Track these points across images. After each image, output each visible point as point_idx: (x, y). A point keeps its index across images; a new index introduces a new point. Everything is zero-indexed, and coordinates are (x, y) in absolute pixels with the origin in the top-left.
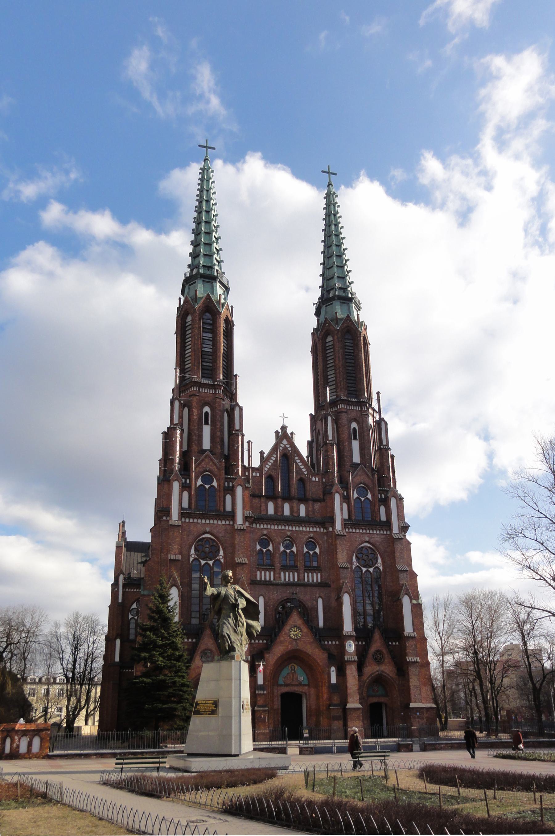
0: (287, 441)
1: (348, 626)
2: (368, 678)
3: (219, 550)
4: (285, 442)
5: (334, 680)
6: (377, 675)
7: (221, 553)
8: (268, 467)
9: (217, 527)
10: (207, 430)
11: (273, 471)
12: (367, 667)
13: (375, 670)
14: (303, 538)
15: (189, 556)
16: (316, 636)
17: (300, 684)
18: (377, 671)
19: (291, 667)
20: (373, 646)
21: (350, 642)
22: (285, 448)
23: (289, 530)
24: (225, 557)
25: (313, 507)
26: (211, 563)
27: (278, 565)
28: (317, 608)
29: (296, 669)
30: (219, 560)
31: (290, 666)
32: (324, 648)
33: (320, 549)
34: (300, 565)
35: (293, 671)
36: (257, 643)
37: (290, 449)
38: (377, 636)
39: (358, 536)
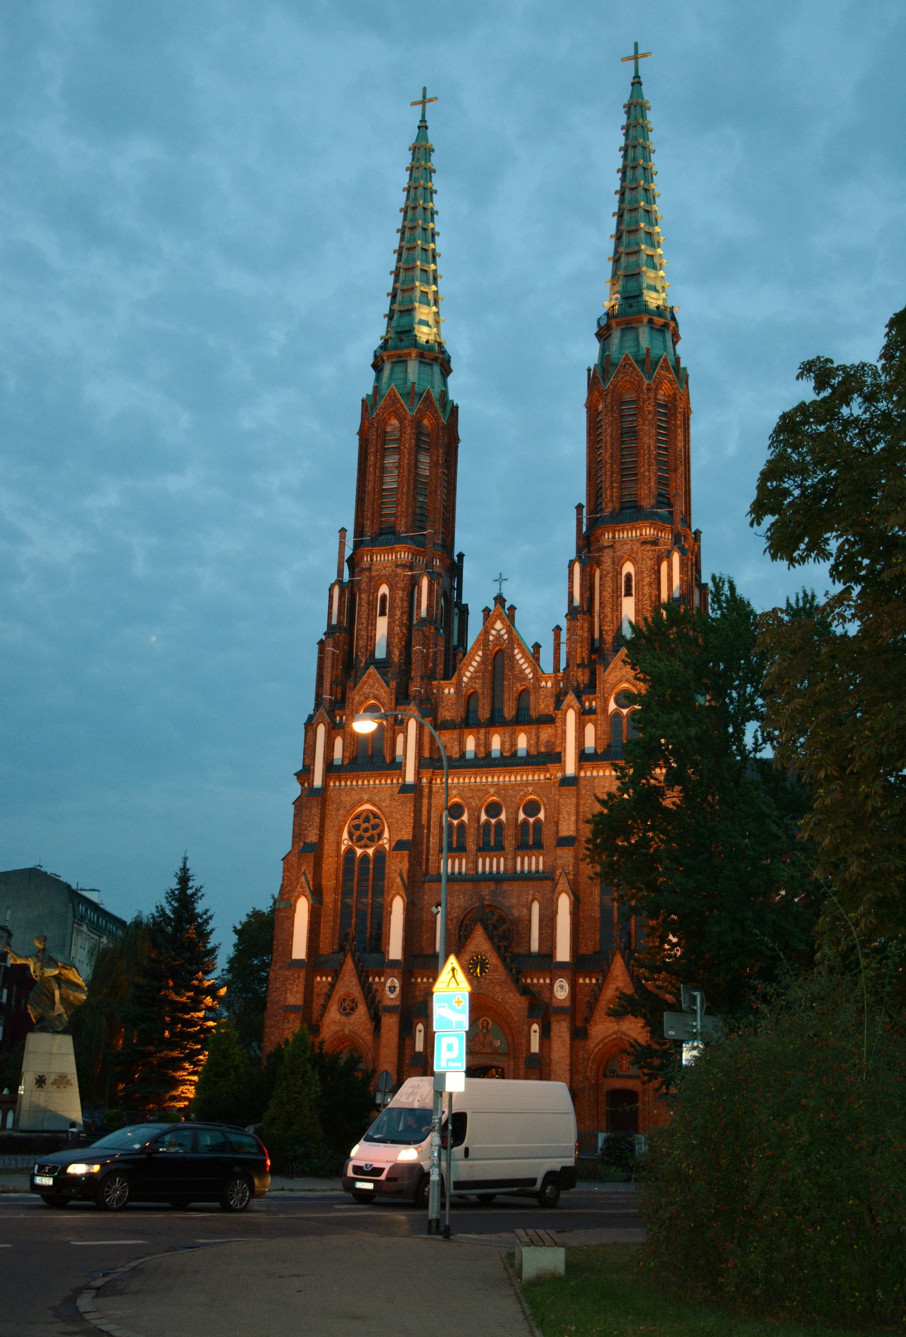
0: (502, 623)
1: (563, 953)
2: (598, 1044)
3: (382, 832)
4: (498, 625)
5: (535, 1048)
6: (613, 1040)
7: (386, 834)
8: (468, 674)
9: (379, 791)
10: (382, 624)
11: (477, 681)
12: (596, 1024)
13: (610, 1031)
14: (515, 796)
15: (339, 843)
16: (511, 971)
17: (495, 1052)
18: (615, 1033)
19: (482, 1024)
20: (611, 986)
21: (561, 981)
22: (499, 637)
23: (492, 785)
24: (390, 841)
25: (538, 738)
26: (370, 851)
27: (471, 846)
28: (530, 921)
29: (489, 1027)
30: (382, 846)
31: (481, 1021)
32: (525, 991)
33: (545, 812)
34: (509, 842)
35: (485, 1031)
36: (425, 983)
37: (506, 637)
38: (618, 966)
39: (607, 785)
